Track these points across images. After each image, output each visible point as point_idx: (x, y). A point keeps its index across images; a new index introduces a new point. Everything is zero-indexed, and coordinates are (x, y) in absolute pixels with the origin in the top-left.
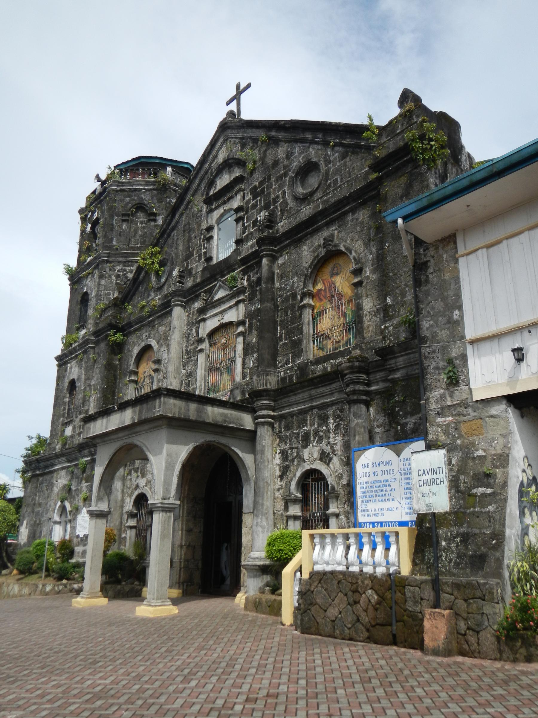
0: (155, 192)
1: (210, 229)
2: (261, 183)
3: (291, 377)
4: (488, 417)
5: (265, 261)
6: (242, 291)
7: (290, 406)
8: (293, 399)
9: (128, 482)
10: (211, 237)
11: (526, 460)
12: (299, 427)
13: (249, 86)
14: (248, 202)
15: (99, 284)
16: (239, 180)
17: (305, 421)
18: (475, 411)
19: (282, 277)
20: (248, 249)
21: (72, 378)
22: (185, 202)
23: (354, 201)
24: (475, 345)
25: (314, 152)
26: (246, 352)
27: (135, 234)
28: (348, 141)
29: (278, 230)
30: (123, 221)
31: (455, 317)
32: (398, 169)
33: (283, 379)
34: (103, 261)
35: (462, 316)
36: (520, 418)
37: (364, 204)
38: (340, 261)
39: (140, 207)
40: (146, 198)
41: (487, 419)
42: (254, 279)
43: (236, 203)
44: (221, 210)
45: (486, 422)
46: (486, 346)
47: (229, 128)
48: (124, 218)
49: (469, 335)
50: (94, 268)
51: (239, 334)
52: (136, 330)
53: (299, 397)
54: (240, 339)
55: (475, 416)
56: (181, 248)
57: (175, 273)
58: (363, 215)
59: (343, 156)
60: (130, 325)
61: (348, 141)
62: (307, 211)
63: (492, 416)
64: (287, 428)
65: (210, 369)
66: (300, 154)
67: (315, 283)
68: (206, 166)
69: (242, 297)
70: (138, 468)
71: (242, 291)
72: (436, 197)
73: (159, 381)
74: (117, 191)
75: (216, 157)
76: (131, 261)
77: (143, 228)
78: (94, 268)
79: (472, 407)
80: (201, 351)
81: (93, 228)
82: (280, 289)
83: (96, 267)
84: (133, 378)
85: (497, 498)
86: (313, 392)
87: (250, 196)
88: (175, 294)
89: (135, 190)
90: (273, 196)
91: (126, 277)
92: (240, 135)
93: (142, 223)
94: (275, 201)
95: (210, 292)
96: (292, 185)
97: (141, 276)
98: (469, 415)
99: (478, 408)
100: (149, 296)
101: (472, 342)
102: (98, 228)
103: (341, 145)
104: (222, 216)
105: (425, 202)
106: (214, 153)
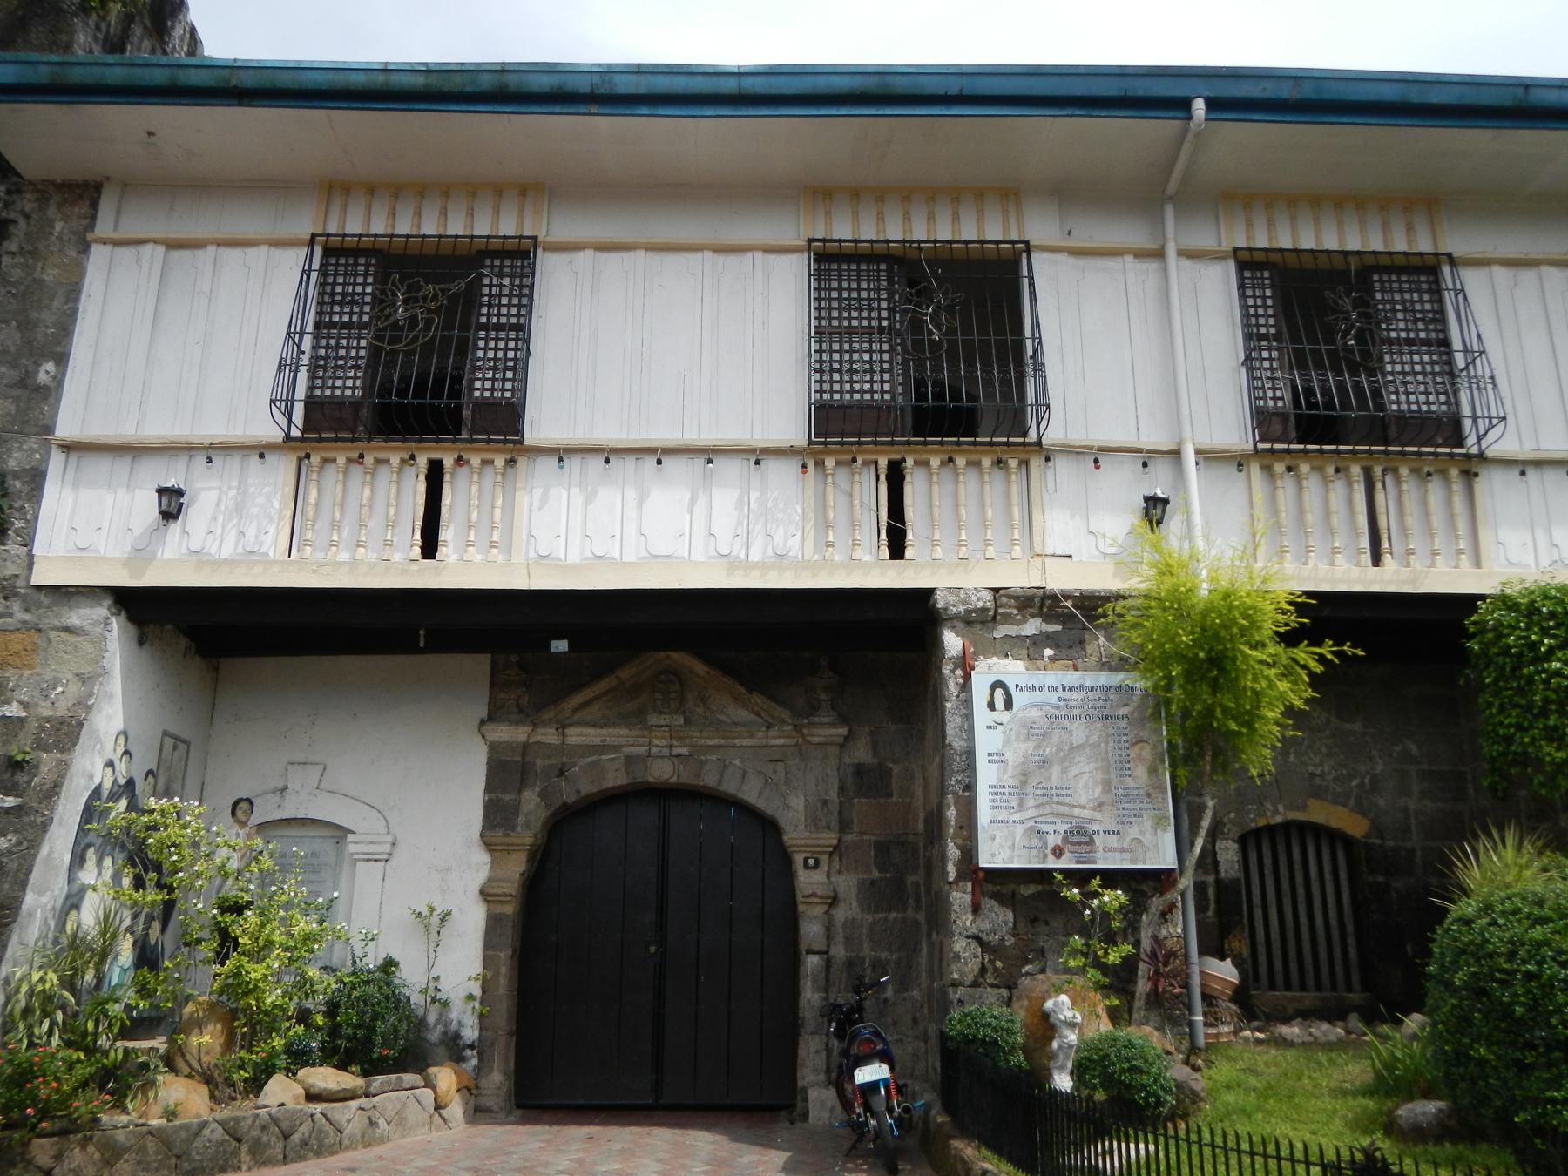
4: (57, 629)
11: (121, 740)
18: (27, 610)
24: (74, 457)
31: (42, 378)
35: (59, 381)
36: (134, 645)
41: (53, 634)
45: (49, 641)
46: (100, 466)
49: (67, 426)
55: (25, 622)
63: (67, 630)
72: (77, 75)
79: (24, 598)
85: (26, 819)
98: (11, 615)
99: (39, 605)
101: (68, 448)
105: (43, 75)
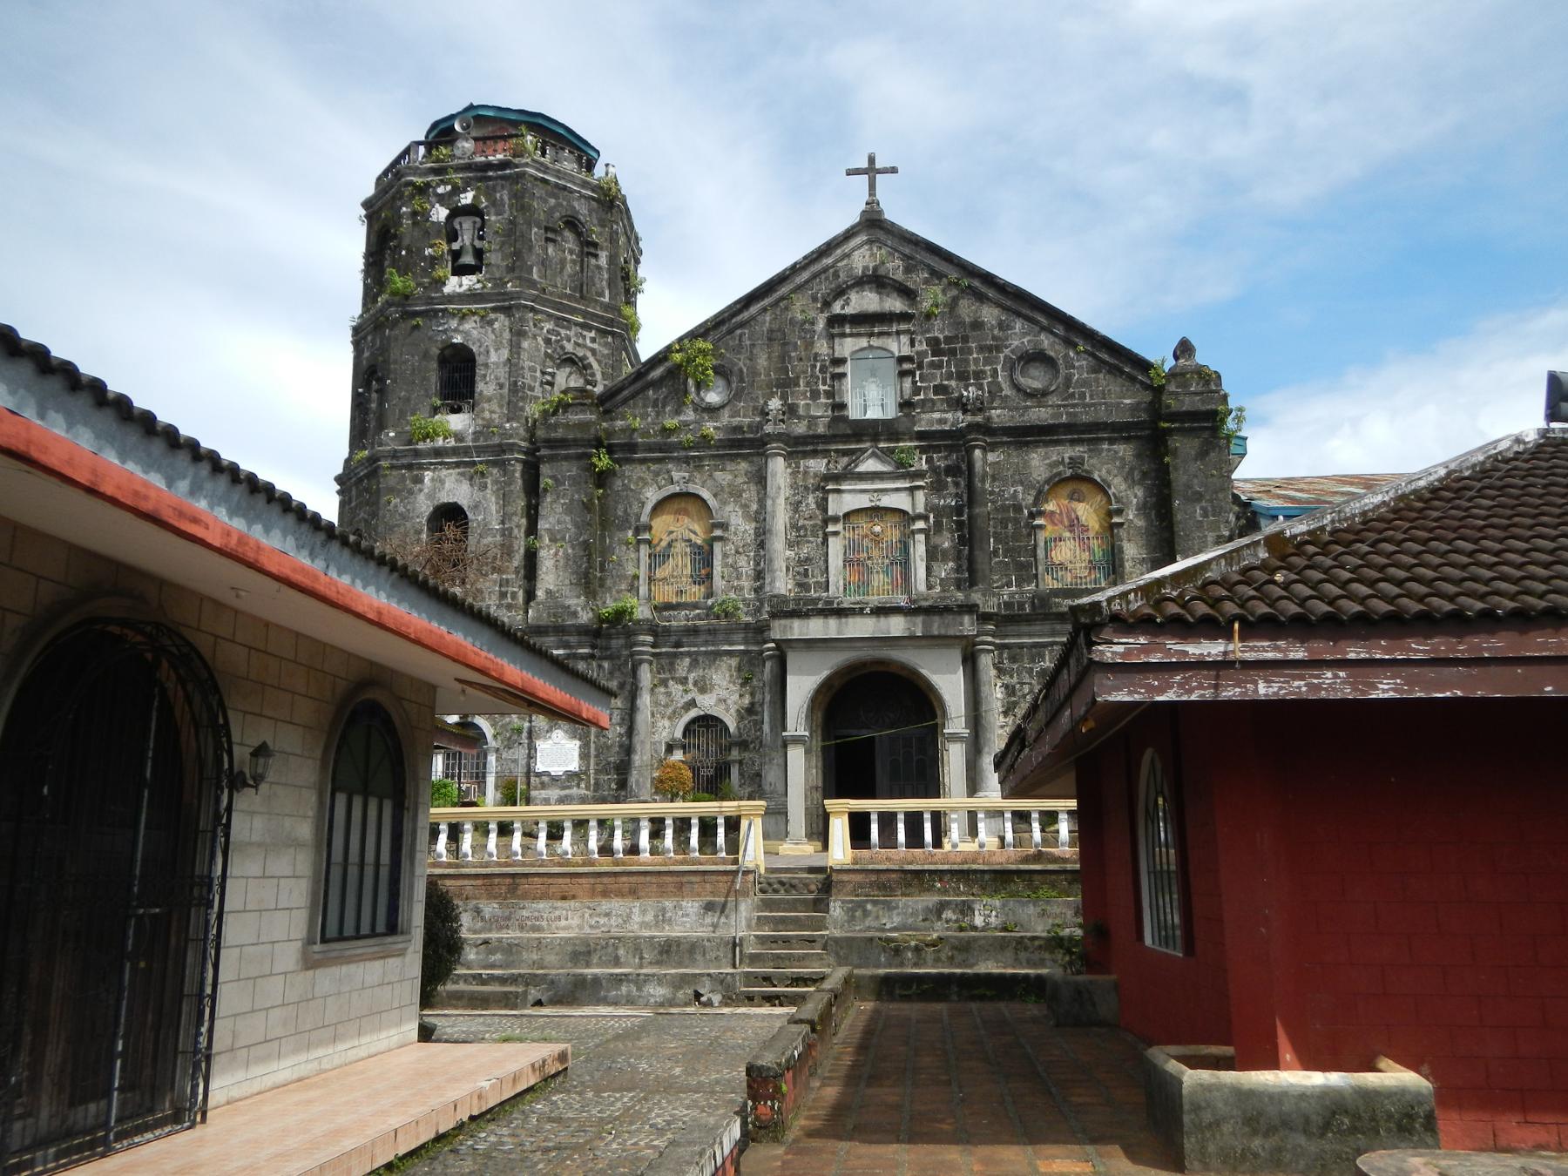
0: (594, 204)
1: (841, 362)
2: (948, 340)
3: (1021, 605)
5: (978, 453)
6: (919, 475)
7: (1019, 636)
8: (1025, 628)
9: (663, 699)
10: (844, 375)
12: (1033, 661)
13: (894, 170)
14: (921, 354)
15: (515, 348)
16: (904, 317)
17: (1042, 658)
19: (994, 479)
20: (931, 422)
21: (445, 498)
22: (776, 295)
23: (1113, 431)
25: (1046, 342)
26: (932, 554)
27: (562, 269)
28: (1106, 357)
29: (989, 419)
30: (548, 240)
32: (1192, 430)
33: (1008, 605)
34: (526, 306)
37: (1127, 440)
38: (1085, 488)
39: (572, 223)
40: (582, 209)
42: (942, 464)
43: (899, 346)
44: (863, 342)
47: (882, 228)
48: (550, 235)
50: (494, 310)
51: (920, 531)
52: (643, 461)
53: (1037, 628)
54: (921, 537)
56: (762, 362)
57: (775, 404)
58: (1124, 450)
59: (1095, 371)
60: (632, 447)
61: (1106, 357)
62: (1040, 415)
64: (1013, 659)
65: (847, 562)
66: (1024, 335)
67: (1047, 501)
68: (828, 261)
69: (921, 483)
70: (686, 678)
71: (919, 475)
73: (725, 556)
74: (536, 179)
75: (848, 256)
76: (568, 321)
77: (573, 261)
78: (494, 310)
80: (836, 533)
81: (449, 218)
82: (991, 493)
83: (507, 311)
84: (647, 536)
86: (1058, 627)
87: (925, 347)
88: (778, 437)
89: (565, 188)
90: (973, 367)
91: (563, 348)
92: (907, 251)
93: (571, 252)
94: (979, 375)
95: (855, 455)
96: (1011, 366)
97: (657, 373)
100: (678, 412)
102: (466, 226)
103: (1093, 355)
104: (862, 349)
106: (847, 248)
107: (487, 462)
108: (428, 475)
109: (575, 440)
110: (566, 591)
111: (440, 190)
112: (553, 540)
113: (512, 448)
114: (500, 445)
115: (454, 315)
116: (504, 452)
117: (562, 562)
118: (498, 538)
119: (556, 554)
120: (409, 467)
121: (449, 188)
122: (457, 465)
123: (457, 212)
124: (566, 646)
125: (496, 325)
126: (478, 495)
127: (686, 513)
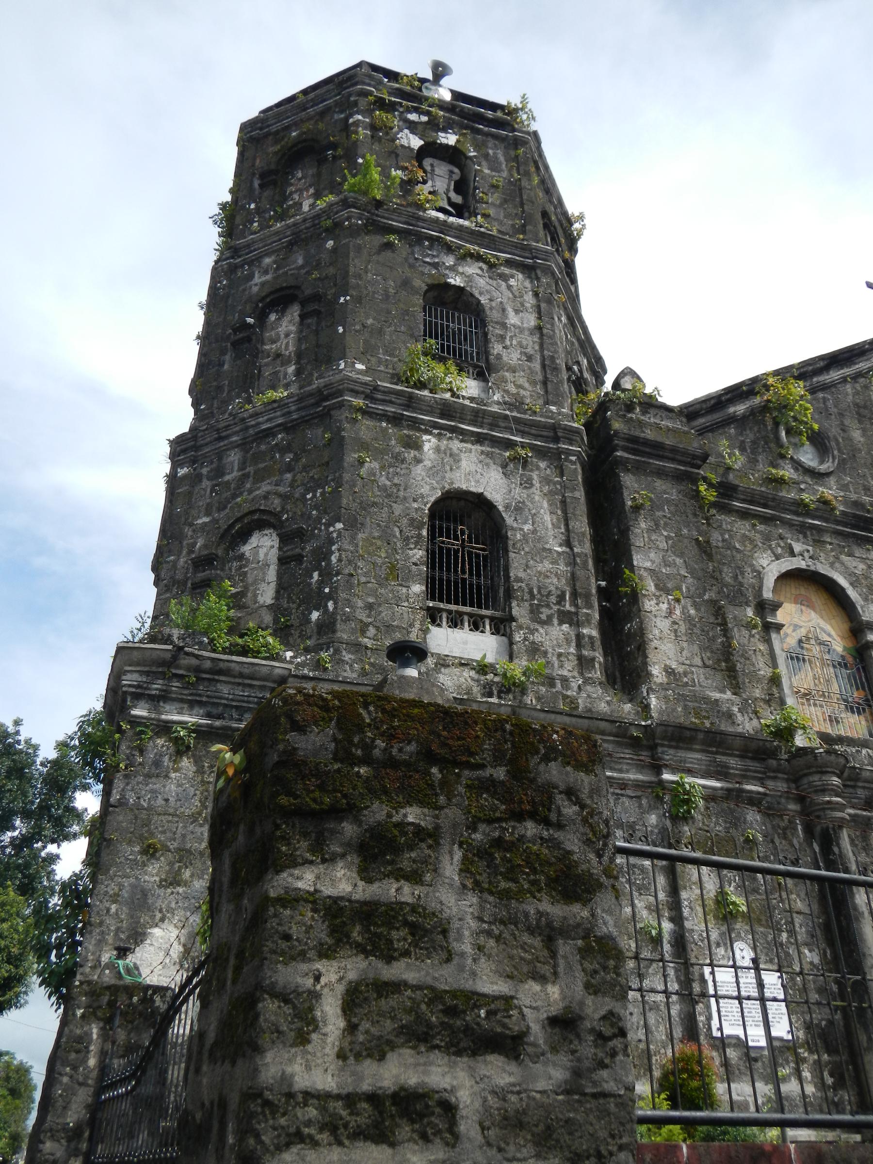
78: (509, 263)
107: (533, 448)
108: (429, 443)
109: (674, 450)
110: (699, 675)
111: (413, 117)
112: (662, 588)
113: (571, 435)
114: (554, 428)
115: (449, 249)
116: (556, 439)
117: (683, 628)
118: (562, 567)
119: (670, 612)
120: (396, 420)
121: (425, 119)
122: (479, 439)
123: (431, 150)
124: (720, 773)
125: (512, 282)
126: (518, 493)
127: (811, 606)
